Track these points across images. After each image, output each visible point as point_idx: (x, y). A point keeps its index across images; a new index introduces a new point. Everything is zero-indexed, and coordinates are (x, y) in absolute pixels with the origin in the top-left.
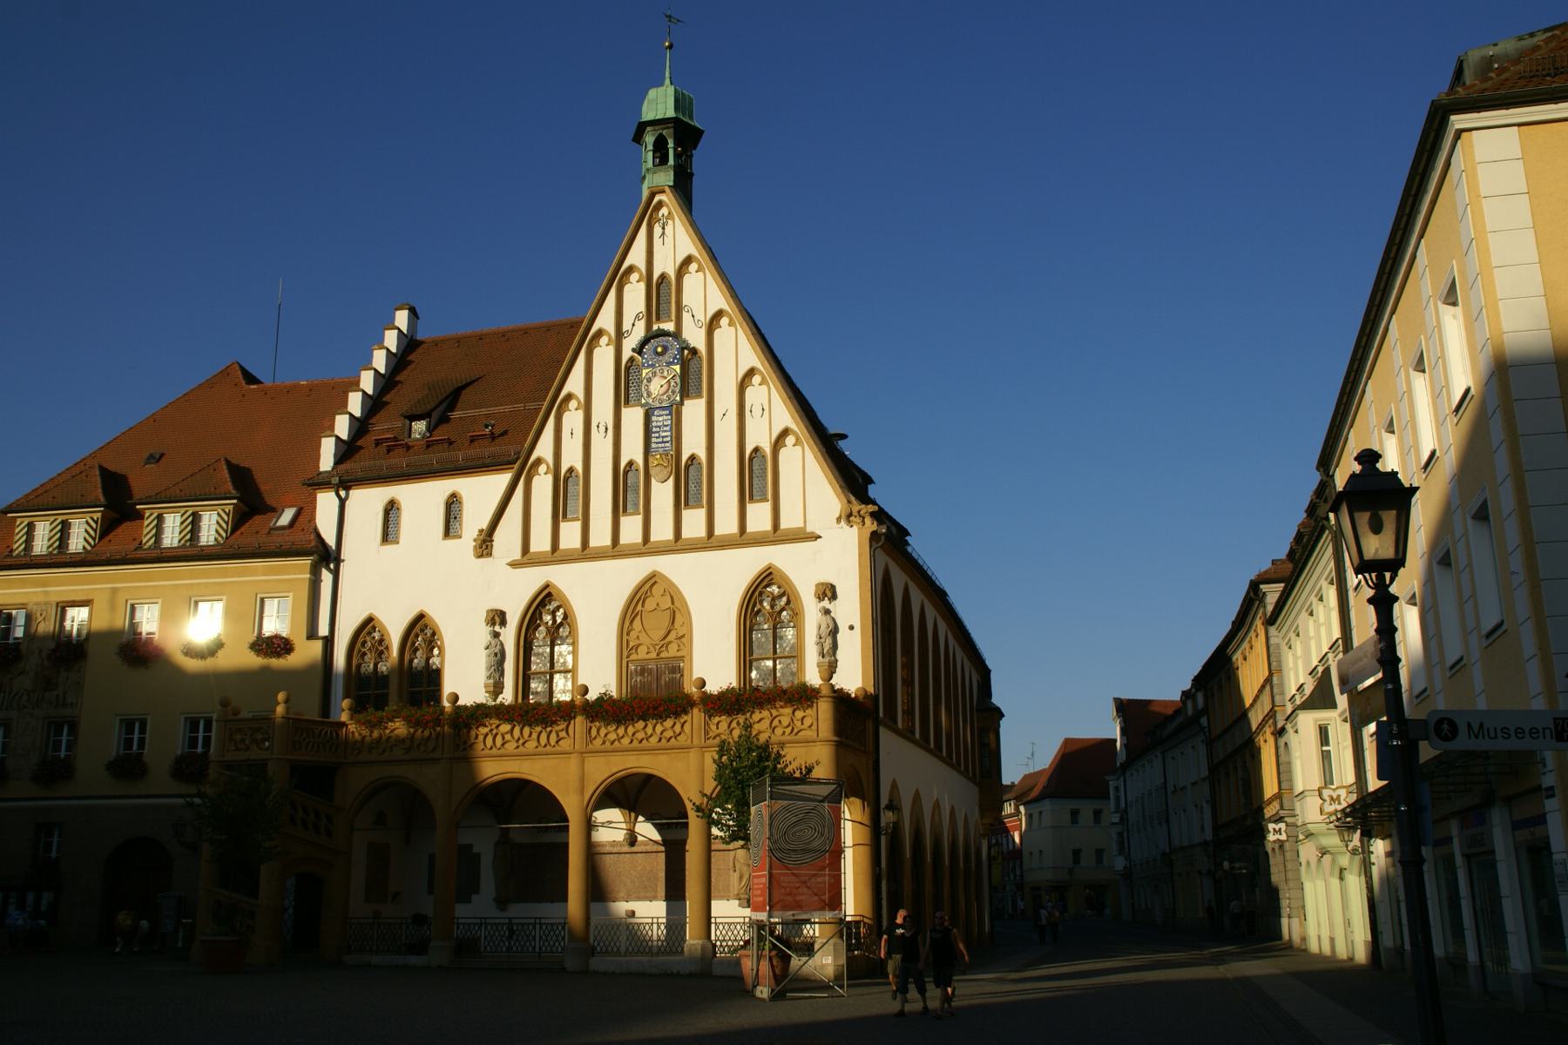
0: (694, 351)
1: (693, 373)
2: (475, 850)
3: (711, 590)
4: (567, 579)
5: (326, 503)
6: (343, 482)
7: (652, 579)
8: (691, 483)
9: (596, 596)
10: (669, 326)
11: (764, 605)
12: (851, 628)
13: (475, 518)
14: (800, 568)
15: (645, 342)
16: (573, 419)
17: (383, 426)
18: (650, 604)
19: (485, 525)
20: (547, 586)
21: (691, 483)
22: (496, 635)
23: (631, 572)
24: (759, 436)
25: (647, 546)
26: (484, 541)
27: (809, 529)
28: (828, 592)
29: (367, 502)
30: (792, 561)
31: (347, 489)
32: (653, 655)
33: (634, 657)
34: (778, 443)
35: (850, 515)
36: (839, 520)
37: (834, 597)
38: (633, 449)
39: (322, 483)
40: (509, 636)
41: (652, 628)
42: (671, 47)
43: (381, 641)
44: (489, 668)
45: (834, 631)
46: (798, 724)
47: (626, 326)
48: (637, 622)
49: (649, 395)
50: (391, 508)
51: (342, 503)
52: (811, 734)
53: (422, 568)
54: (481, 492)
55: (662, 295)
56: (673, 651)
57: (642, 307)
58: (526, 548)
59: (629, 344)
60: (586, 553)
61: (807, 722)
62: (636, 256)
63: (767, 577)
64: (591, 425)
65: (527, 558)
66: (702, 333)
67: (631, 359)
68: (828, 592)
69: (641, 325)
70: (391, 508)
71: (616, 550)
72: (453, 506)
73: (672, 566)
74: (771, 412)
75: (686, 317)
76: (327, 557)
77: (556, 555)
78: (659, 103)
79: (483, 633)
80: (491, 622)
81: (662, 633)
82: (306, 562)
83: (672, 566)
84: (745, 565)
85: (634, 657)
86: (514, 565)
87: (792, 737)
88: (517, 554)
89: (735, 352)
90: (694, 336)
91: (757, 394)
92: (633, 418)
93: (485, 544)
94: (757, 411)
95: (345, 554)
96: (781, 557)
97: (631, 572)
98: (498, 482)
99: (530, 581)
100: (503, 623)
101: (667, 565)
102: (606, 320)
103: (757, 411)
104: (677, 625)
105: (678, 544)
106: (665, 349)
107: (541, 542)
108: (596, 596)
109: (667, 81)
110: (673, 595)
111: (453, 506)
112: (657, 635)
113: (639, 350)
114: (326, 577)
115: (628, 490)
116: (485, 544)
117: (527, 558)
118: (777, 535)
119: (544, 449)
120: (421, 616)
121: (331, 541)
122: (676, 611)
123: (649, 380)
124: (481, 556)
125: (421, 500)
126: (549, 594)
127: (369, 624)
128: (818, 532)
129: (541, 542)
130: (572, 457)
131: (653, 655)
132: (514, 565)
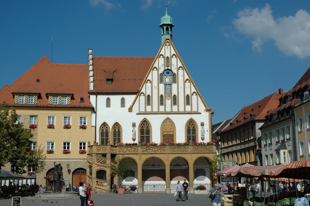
4: (149, 118)
7: (168, 119)
10: (169, 68)
12: (207, 131)
15: (165, 70)
16: (149, 85)
21: (175, 100)
24: (188, 92)
27: (199, 111)
29: (102, 99)
36: (205, 110)
37: (204, 125)
38: (162, 92)
40: (137, 129)
42: (167, 6)
43: (107, 128)
47: (160, 66)
49: (166, 82)
50: (108, 100)
51: (96, 97)
54: (129, 99)
55: (168, 60)
56: (171, 133)
57: (163, 63)
62: (162, 52)
64: (153, 86)
66: (176, 70)
67: (161, 74)
70: (108, 100)
72: (123, 100)
75: (173, 67)
77: (146, 113)
78: (167, 19)
79: (132, 128)
81: (169, 129)
84: (187, 117)
86: (137, 114)
89: (182, 75)
90: (175, 71)
92: (162, 86)
93: (130, 110)
94: (188, 87)
96: (194, 117)
98: (134, 97)
99: (142, 117)
101: (170, 116)
109: (166, 14)
113: (163, 72)
116: (130, 110)
119: (143, 90)
123: (166, 79)
125: (116, 99)
127: (104, 124)
128: (201, 112)
130: (149, 93)
132: (137, 114)
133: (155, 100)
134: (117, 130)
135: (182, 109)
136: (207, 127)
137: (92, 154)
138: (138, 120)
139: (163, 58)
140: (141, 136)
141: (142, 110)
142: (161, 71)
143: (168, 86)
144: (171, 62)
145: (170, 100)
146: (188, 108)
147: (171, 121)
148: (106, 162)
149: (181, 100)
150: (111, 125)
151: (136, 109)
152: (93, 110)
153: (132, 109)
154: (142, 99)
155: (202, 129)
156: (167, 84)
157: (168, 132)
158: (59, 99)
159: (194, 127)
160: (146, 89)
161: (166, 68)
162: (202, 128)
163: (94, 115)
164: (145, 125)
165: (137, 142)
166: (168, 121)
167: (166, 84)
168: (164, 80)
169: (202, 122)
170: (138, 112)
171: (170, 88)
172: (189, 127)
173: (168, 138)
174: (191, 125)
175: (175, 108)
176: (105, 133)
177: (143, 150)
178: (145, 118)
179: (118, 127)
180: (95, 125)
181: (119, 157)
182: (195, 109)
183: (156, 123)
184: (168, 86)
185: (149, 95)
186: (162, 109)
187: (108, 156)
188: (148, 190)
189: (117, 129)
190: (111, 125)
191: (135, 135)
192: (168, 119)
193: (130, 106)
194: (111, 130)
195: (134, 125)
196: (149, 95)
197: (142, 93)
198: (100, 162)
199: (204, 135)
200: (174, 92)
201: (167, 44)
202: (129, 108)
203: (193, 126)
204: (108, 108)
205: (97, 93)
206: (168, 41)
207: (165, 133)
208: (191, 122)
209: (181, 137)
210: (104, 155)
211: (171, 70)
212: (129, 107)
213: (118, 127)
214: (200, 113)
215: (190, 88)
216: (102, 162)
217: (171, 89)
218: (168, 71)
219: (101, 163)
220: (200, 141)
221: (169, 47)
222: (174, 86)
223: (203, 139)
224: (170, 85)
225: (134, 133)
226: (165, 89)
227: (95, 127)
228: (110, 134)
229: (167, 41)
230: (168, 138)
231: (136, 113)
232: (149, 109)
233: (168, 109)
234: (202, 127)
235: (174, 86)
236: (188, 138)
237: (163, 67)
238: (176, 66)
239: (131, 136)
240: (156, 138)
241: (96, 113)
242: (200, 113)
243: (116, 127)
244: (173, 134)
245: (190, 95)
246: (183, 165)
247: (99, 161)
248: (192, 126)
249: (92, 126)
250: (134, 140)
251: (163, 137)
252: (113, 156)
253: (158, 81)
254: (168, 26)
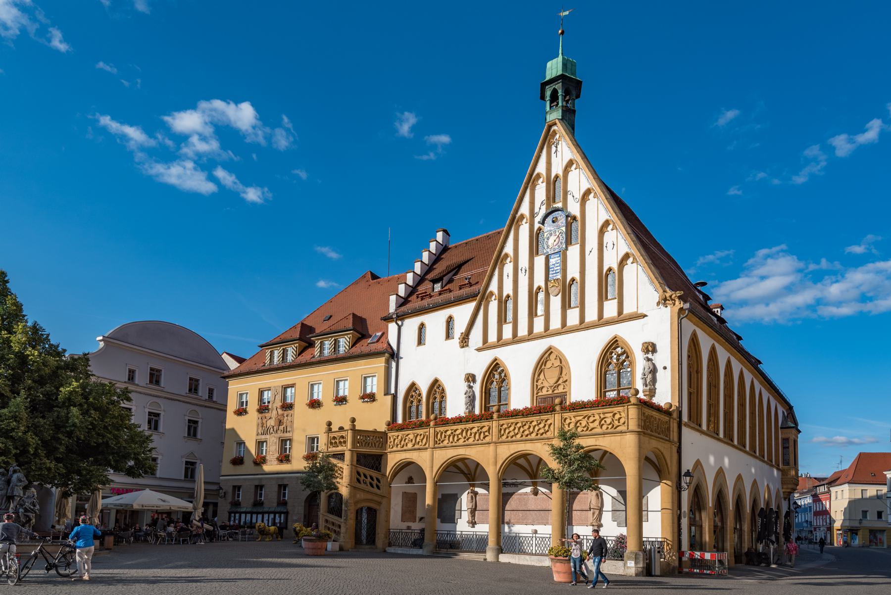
0: (574, 218)
1: (573, 229)
3: (581, 355)
5: (392, 327)
6: (401, 317)
7: (549, 351)
9: (519, 362)
11: (613, 358)
13: (460, 327)
14: (633, 335)
16: (508, 268)
17: (426, 287)
18: (549, 364)
19: (463, 330)
20: (496, 359)
22: (470, 387)
23: (537, 348)
25: (548, 332)
26: (464, 338)
27: (640, 311)
28: (650, 348)
29: (411, 325)
31: (402, 320)
32: (550, 392)
33: (540, 394)
34: (622, 263)
35: (665, 299)
36: (658, 304)
40: (477, 388)
41: (550, 377)
44: (466, 404)
45: (654, 371)
46: (616, 423)
47: (536, 210)
48: (542, 376)
50: (422, 327)
52: (623, 428)
53: (437, 354)
54: (462, 313)
57: (544, 198)
58: (485, 340)
59: (538, 219)
60: (516, 339)
61: (622, 421)
62: (541, 168)
63: (614, 343)
65: (486, 346)
66: (578, 205)
67: (540, 229)
68: (650, 348)
69: (544, 208)
70: (422, 327)
71: (531, 336)
72: (450, 320)
73: (559, 343)
74: (619, 242)
76: (393, 355)
77: (501, 343)
80: (467, 380)
81: (555, 379)
82: (383, 359)
83: (559, 343)
84: (601, 337)
85: (540, 394)
86: (479, 350)
87: (612, 430)
88: (480, 345)
91: (610, 236)
92: (540, 261)
94: (610, 246)
95: (402, 354)
96: (622, 330)
97: (537, 348)
99: (487, 357)
100: (474, 381)
102: (525, 209)
103: (610, 246)
104: (563, 375)
105: (565, 329)
107: (493, 338)
108: (519, 362)
110: (561, 359)
112: (552, 381)
114: (394, 364)
117: (486, 346)
118: (621, 318)
120: (436, 381)
121: (395, 347)
122: (562, 367)
123: (548, 239)
124: (463, 347)
125: (435, 321)
126: (497, 364)
129: (493, 338)
131: (550, 392)
132: (479, 350)
138: (479, 364)
147: (560, 352)
154: (493, 306)
190: (424, 389)
204: (421, 347)
214: (645, 316)
218: (554, 215)
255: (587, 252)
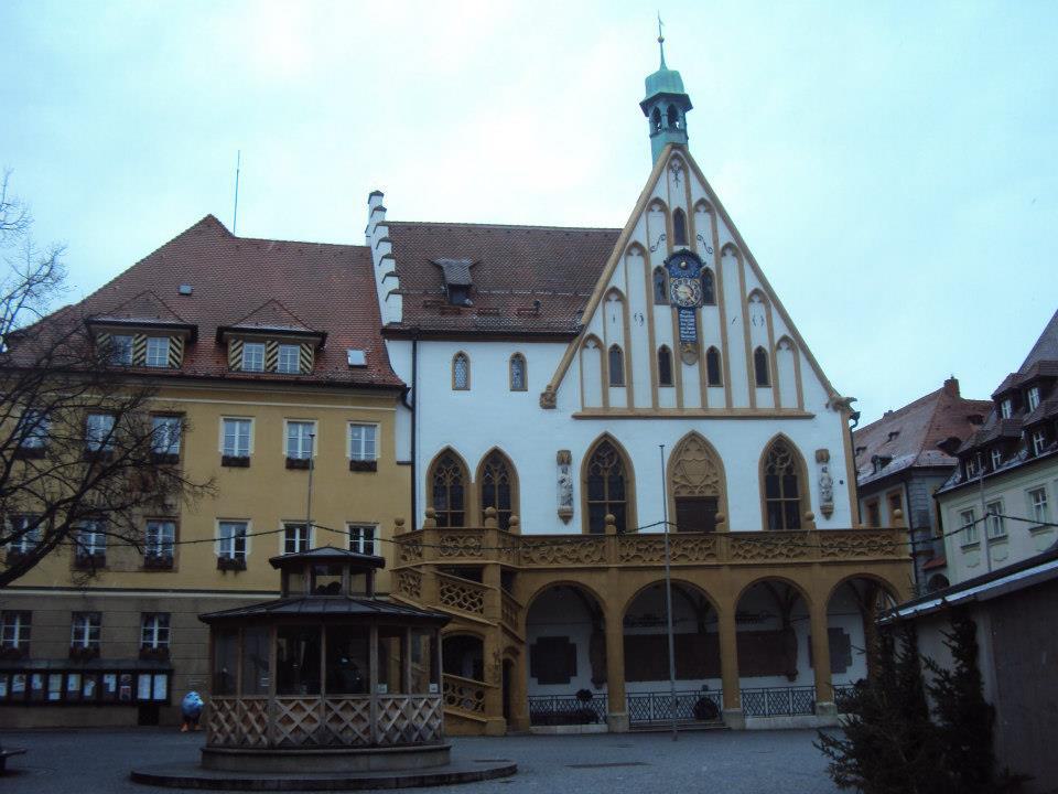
0: (707, 270)
2: (571, 641)
4: (624, 433)
7: (693, 437)
8: (714, 371)
10: (688, 248)
12: (841, 482)
15: (674, 257)
16: (614, 308)
21: (714, 371)
27: (808, 409)
30: (796, 433)
36: (827, 406)
38: (665, 336)
39: (393, 333)
40: (576, 475)
47: (653, 243)
49: (677, 297)
54: (543, 361)
56: (709, 493)
66: (712, 257)
67: (658, 269)
72: (518, 361)
79: (554, 473)
83: (711, 431)
84: (764, 433)
86: (577, 417)
90: (709, 260)
92: (664, 314)
93: (549, 401)
94: (758, 321)
97: (674, 433)
99: (591, 432)
103: (758, 321)
106: (686, 267)
111: (518, 361)
115: (665, 372)
116: (549, 401)
123: (676, 287)
125: (490, 360)
128: (813, 413)
130: (614, 337)
132: (577, 417)
133: (642, 367)
134: (497, 480)
135: (741, 402)
136: (839, 467)
137: (420, 566)
138: (581, 440)
139: (662, 214)
140: (589, 504)
141: (595, 402)
142: (659, 258)
143: (687, 313)
144: (693, 231)
145: (696, 367)
146: (765, 398)
148: (481, 601)
149: (738, 368)
150: (473, 460)
151: (569, 399)
152: (401, 395)
153: (554, 395)
155: (824, 474)
156: (684, 308)
157: (696, 487)
158: (270, 351)
159: (789, 470)
160: (605, 323)
161: (678, 248)
162: (824, 470)
163: (403, 418)
164: (607, 461)
165: (576, 527)
166: (693, 447)
167: (680, 308)
168: (671, 290)
169: (820, 447)
170: (578, 410)
171: (693, 320)
172: (771, 470)
173: (697, 510)
174: (778, 460)
175: (716, 397)
176: (449, 490)
177: (624, 554)
178: (606, 435)
179: (499, 467)
180: (407, 457)
181: (528, 589)
182: (789, 403)
183: (649, 454)
184: (687, 316)
185: (615, 347)
186: (667, 397)
187: (492, 579)
188: (652, 717)
189: (497, 474)
190: (473, 460)
191: (569, 500)
192: (693, 437)
193: (549, 387)
194: (473, 480)
195: (564, 459)
196: (615, 347)
197: (592, 337)
198: (457, 601)
199: (830, 500)
200: (711, 338)
201: (673, 164)
202: (543, 395)
203: (785, 465)
205: (413, 334)
206: (679, 152)
207: (684, 493)
208: (779, 449)
209: (744, 511)
210: (475, 573)
211: (692, 257)
212: (544, 390)
213: (499, 467)
214: (810, 417)
215: (764, 317)
216: (465, 601)
217: (697, 326)
219: (460, 606)
220: (821, 523)
221: (681, 176)
222: (709, 314)
223: (827, 512)
224: (694, 309)
225: (564, 492)
226: (678, 324)
227: (409, 468)
228: (474, 491)
229: (673, 152)
230: (697, 510)
231: (573, 412)
232: (618, 398)
233: (692, 402)
234: (821, 466)
235: (709, 314)
236: (772, 510)
237: (664, 245)
238: (710, 244)
239: (554, 505)
240: (651, 510)
241: (412, 409)
242: (810, 417)
243: (492, 468)
244: (714, 495)
245: (767, 348)
246: (765, 613)
247: (453, 599)
248: (782, 464)
249: (399, 463)
250: (566, 517)
251: (677, 507)
252: (508, 575)
253: (648, 297)
254: (675, 104)
255: (729, 320)
